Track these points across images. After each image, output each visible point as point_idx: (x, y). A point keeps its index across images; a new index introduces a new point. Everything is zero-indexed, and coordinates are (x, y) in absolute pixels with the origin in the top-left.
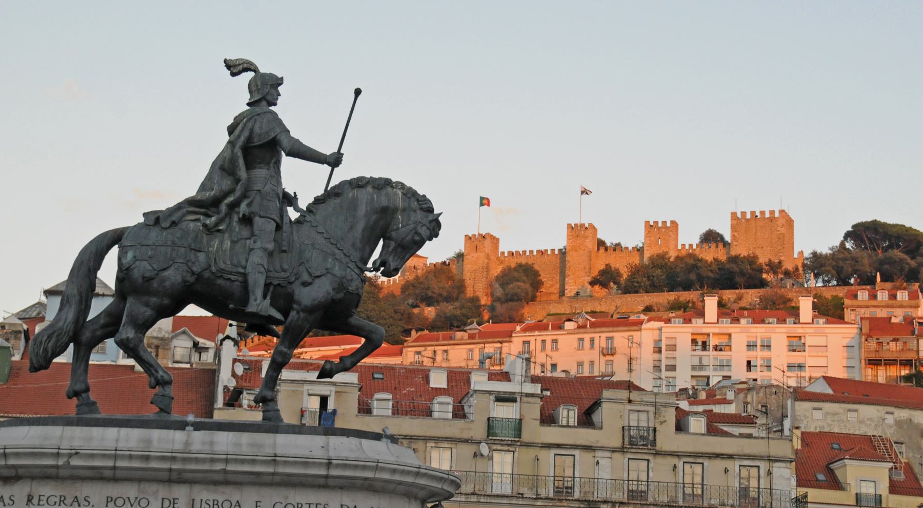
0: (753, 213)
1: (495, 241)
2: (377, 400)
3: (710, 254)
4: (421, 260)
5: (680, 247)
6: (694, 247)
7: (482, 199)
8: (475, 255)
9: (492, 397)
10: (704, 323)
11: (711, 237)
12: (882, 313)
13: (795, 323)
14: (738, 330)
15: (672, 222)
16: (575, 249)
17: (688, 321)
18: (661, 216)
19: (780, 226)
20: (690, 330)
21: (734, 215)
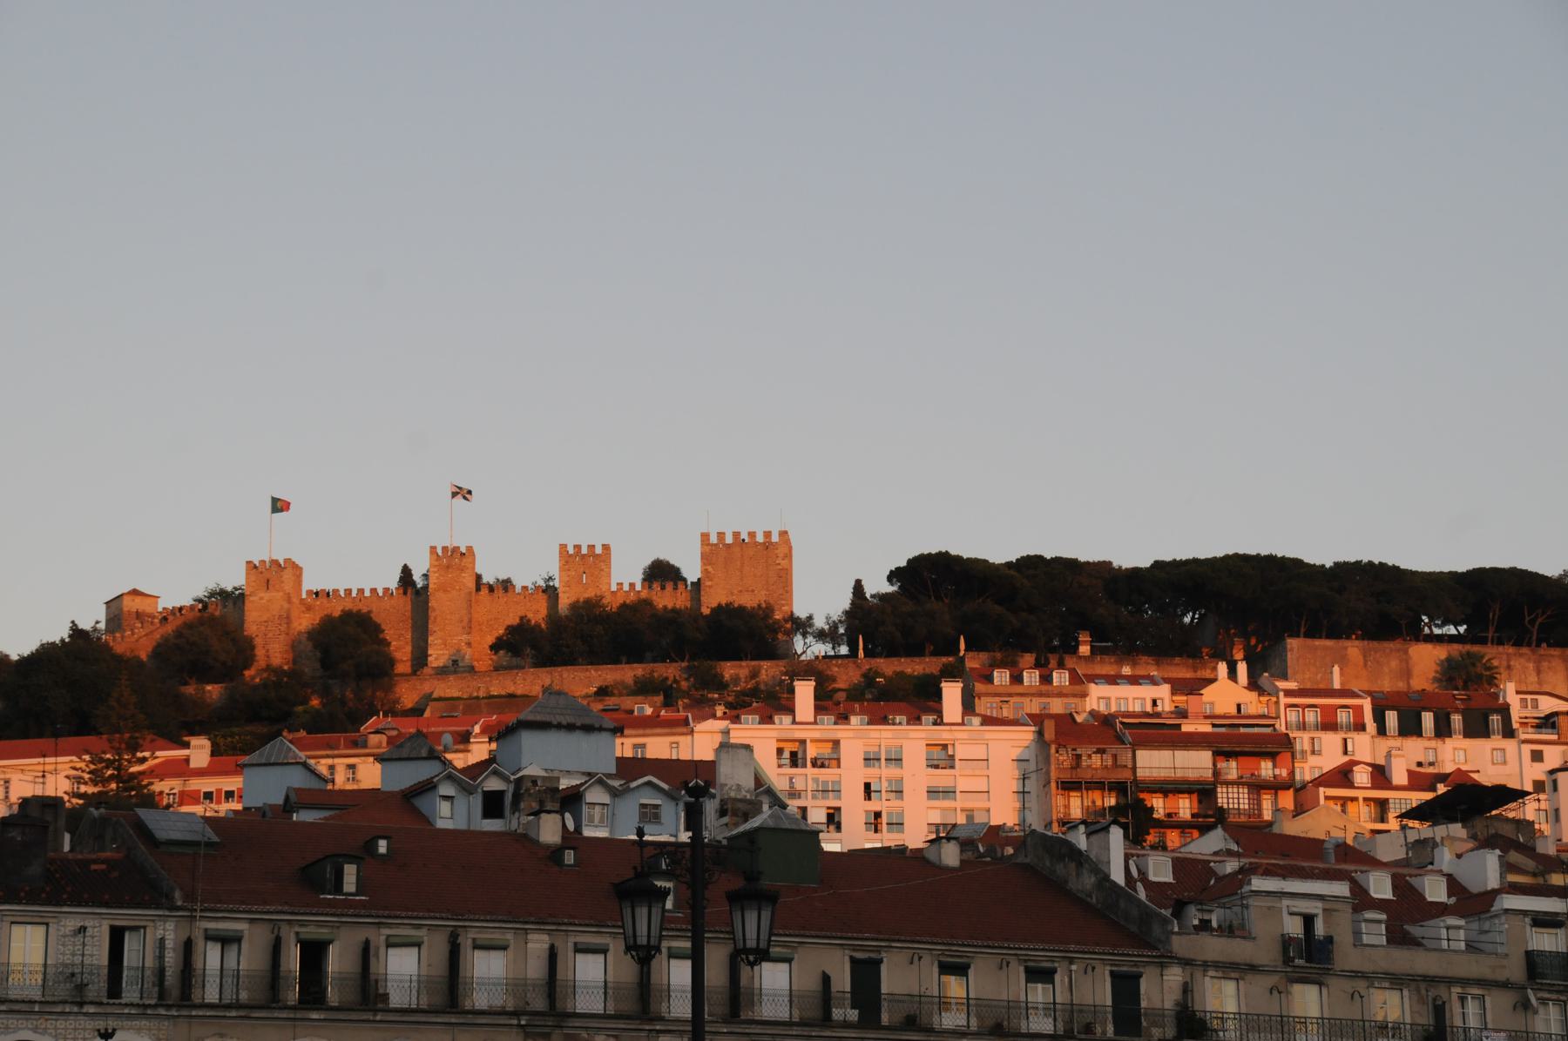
0: (736, 535)
1: (297, 570)
2: (1367, 921)
3: (666, 599)
4: (149, 600)
5: (614, 588)
6: (638, 587)
7: (275, 501)
8: (266, 596)
9: (1528, 920)
10: (794, 722)
11: (661, 572)
12: (1057, 706)
13: (935, 724)
14: (851, 734)
15: (606, 547)
16: (443, 588)
17: (767, 719)
18: (586, 537)
19: (770, 555)
20: (775, 734)
21: (705, 537)
